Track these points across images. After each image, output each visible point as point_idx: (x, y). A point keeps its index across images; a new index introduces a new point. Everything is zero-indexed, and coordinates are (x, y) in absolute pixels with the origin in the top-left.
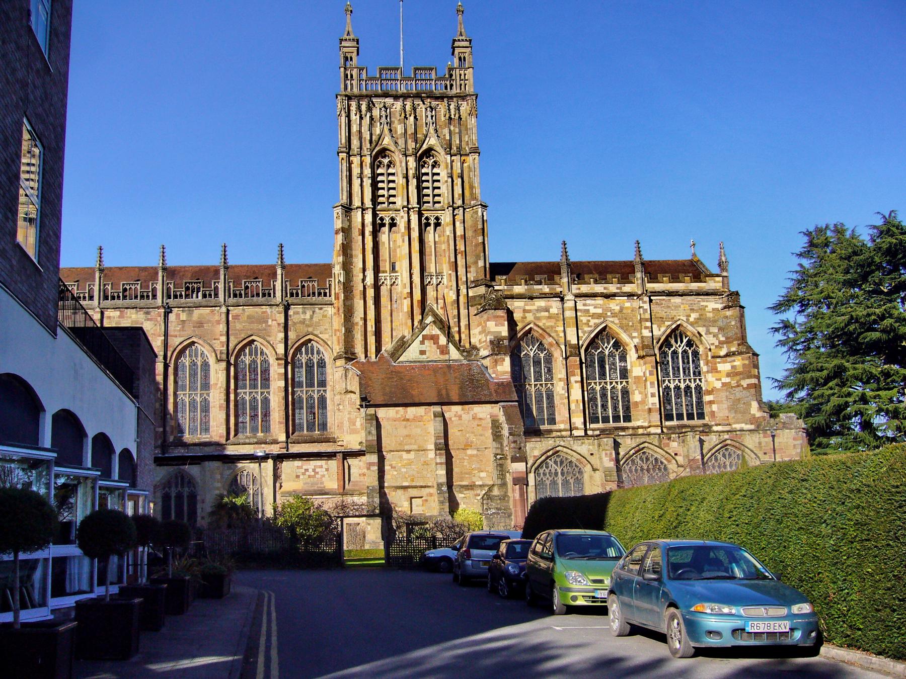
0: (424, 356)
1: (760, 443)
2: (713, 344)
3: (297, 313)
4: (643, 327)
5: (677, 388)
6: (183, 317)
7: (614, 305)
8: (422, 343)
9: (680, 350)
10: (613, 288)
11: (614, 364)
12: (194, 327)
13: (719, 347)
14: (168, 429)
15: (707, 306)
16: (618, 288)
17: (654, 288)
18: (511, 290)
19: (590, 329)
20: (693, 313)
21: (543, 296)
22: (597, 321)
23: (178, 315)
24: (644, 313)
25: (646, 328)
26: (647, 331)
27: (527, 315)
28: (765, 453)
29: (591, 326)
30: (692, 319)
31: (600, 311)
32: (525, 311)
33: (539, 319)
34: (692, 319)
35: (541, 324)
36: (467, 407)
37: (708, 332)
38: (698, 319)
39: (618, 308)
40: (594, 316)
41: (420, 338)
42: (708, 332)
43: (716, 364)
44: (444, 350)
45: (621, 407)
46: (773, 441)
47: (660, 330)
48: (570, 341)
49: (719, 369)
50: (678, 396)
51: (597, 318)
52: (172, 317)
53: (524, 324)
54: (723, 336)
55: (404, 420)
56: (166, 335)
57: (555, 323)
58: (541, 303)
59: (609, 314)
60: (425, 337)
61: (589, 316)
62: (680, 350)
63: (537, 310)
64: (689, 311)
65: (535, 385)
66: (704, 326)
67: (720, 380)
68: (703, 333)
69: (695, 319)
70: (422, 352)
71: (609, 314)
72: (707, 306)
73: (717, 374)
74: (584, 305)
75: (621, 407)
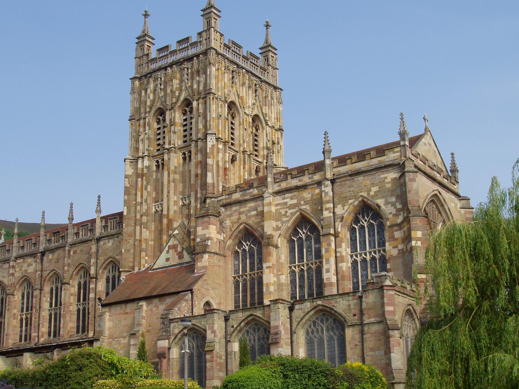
0: (169, 262)
1: (349, 306)
2: (391, 213)
3: (105, 244)
4: (324, 209)
6: (50, 256)
7: (307, 195)
8: (168, 252)
9: (366, 224)
10: (306, 179)
12: (55, 263)
13: (396, 215)
14: (40, 334)
15: (386, 178)
16: (310, 178)
17: (340, 170)
18: (231, 198)
19: (287, 219)
20: (374, 187)
22: (292, 211)
23: (48, 256)
24: (325, 196)
25: (327, 209)
26: (328, 212)
27: (241, 216)
28: (354, 315)
29: (288, 217)
30: (372, 193)
31: (295, 201)
32: (240, 213)
33: (249, 217)
34: (372, 193)
36: (162, 298)
37: (387, 203)
38: (378, 191)
39: (310, 195)
40: (291, 207)
41: (167, 248)
43: (393, 232)
45: (314, 286)
46: (361, 302)
47: (344, 209)
48: (266, 232)
49: (396, 237)
50: (364, 269)
51: (293, 208)
52: (45, 258)
53: (239, 224)
54: (400, 204)
55: (124, 314)
56: (42, 271)
57: (261, 219)
58: (252, 204)
59: (302, 202)
60: (170, 248)
61: (287, 208)
62: (366, 224)
63: (249, 211)
64: (370, 186)
65: (250, 275)
66: (383, 197)
67: (397, 247)
68: (382, 205)
69: (375, 192)
70: (168, 260)
71: (302, 202)
72: (386, 178)
73: (394, 242)
74: (283, 199)
75: (314, 286)
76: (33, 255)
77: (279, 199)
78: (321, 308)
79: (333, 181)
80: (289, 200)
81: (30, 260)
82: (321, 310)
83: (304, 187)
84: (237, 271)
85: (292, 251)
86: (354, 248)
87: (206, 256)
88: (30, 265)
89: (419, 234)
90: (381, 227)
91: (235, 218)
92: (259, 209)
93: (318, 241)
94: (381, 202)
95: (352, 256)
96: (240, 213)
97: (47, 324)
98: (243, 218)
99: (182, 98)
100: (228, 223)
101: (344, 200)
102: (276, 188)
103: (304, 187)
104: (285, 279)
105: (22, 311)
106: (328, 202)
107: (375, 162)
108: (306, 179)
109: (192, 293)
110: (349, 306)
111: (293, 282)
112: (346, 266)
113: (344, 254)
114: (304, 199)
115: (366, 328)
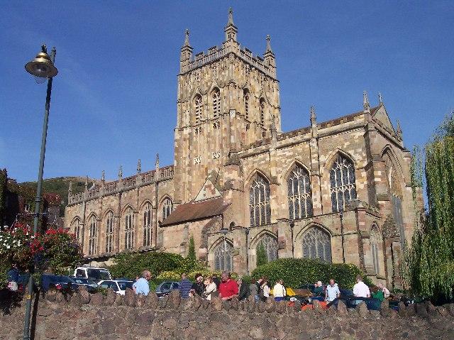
1: (333, 222)
5: (340, 193)
7: (299, 148)
10: (299, 138)
11: (302, 184)
21: (263, 152)
22: (289, 160)
25: (314, 158)
30: (345, 147)
31: (291, 154)
32: (254, 163)
33: (260, 165)
34: (345, 147)
35: (261, 168)
37: (356, 153)
42: (356, 153)
44: (213, 192)
46: (341, 220)
50: (340, 198)
56: (120, 204)
58: (262, 156)
63: (260, 161)
68: (352, 154)
70: (205, 195)
76: (114, 194)
77: (280, 152)
78: (312, 224)
79: (317, 139)
80: (288, 152)
81: (112, 197)
82: (313, 226)
83: (298, 143)
84: (252, 202)
85: (290, 188)
86: (333, 186)
87: (231, 192)
88: (112, 201)
89: (379, 173)
90: (353, 171)
91: (250, 166)
92: (268, 159)
93: (308, 180)
94: (351, 152)
95: (331, 190)
96: (254, 163)
97: (124, 240)
98: (256, 166)
99: (212, 87)
100: (245, 169)
101: (326, 152)
102: (278, 144)
103: (298, 143)
104: (285, 206)
105: (107, 232)
106: (314, 153)
107: (347, 124)
108: (299, 138)
109: (223, 216)
110: (333, 222)
111: (291, 208)
112: (327, 197)
113: (326, 188)
114: (297, 151)
115: (345, 237)
